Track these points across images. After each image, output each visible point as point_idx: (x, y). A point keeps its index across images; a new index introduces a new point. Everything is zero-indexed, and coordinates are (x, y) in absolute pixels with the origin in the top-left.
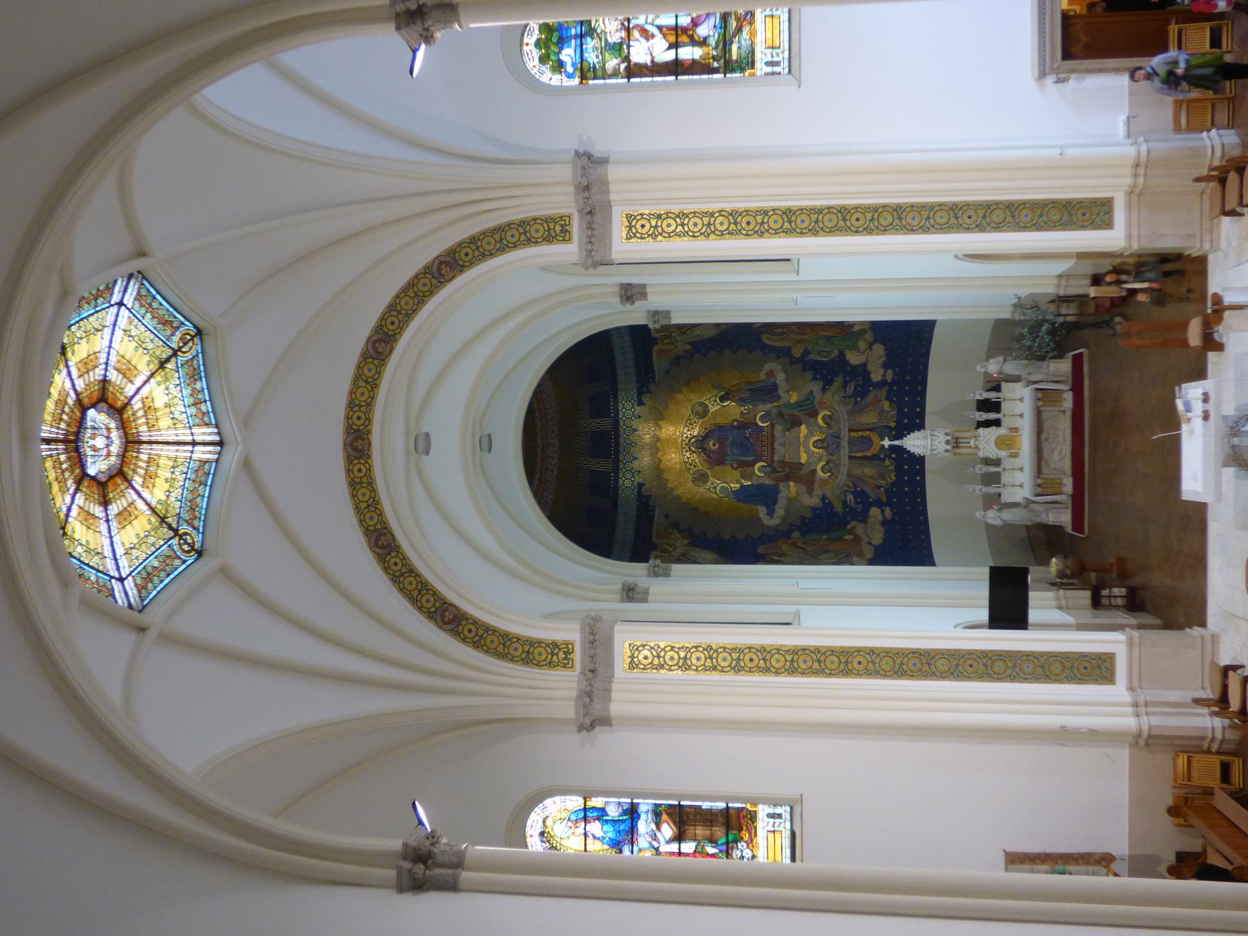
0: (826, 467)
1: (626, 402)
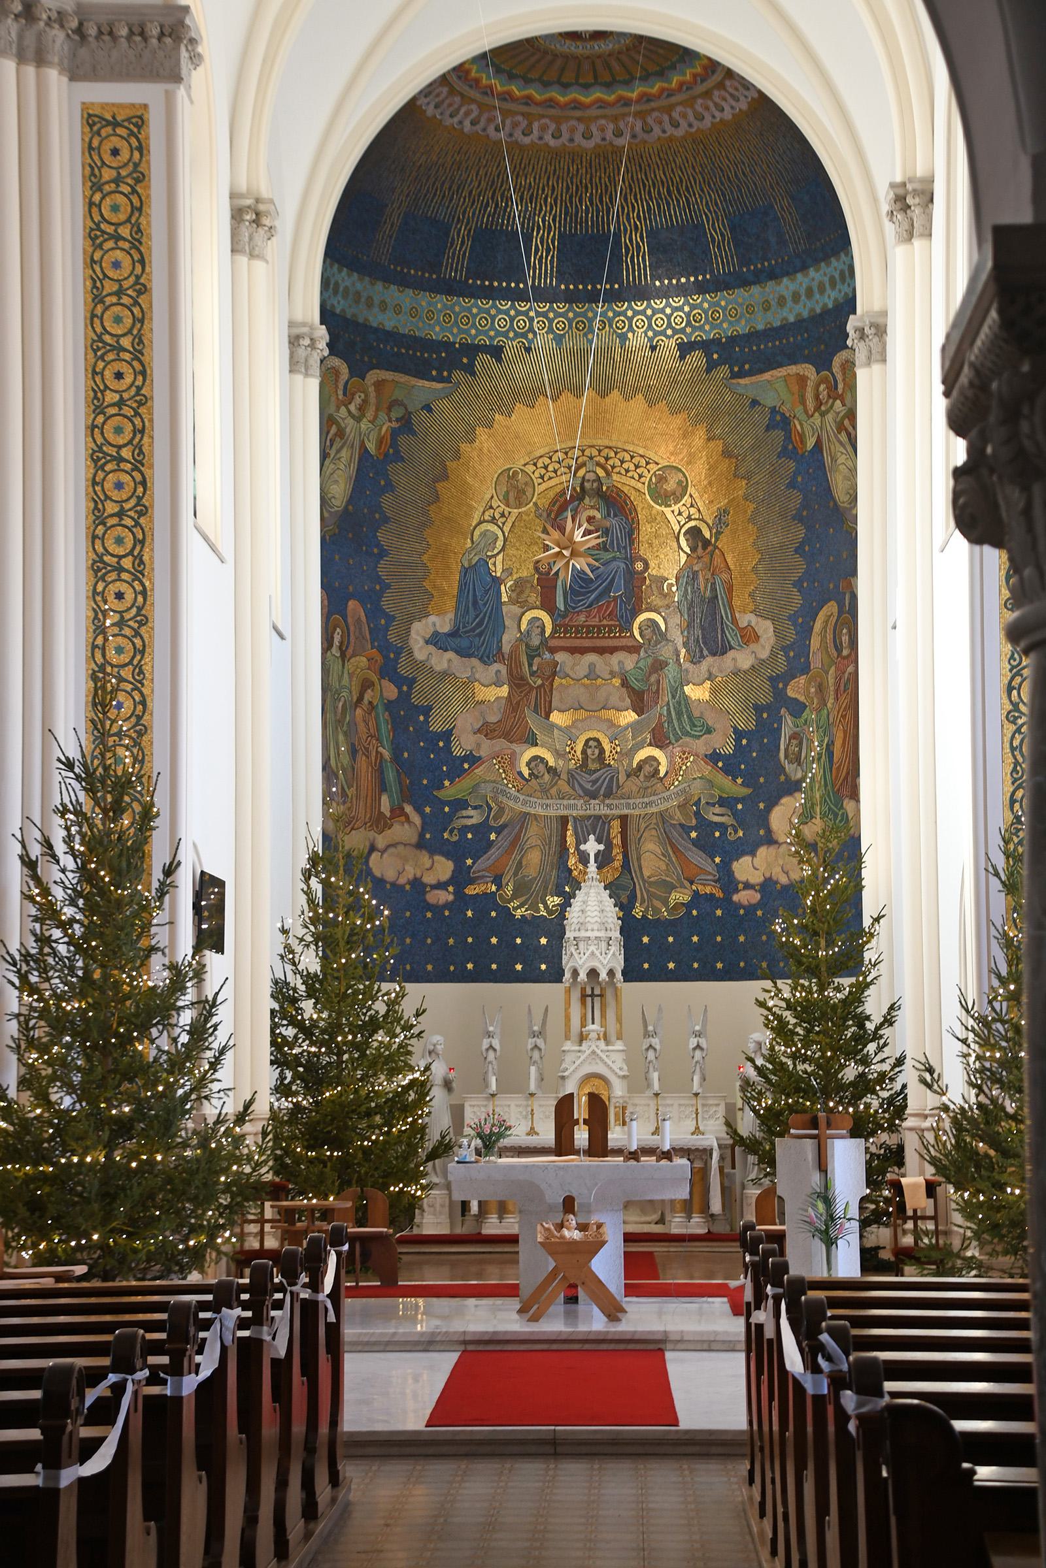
0: (542, 767)
1: (688, 315)
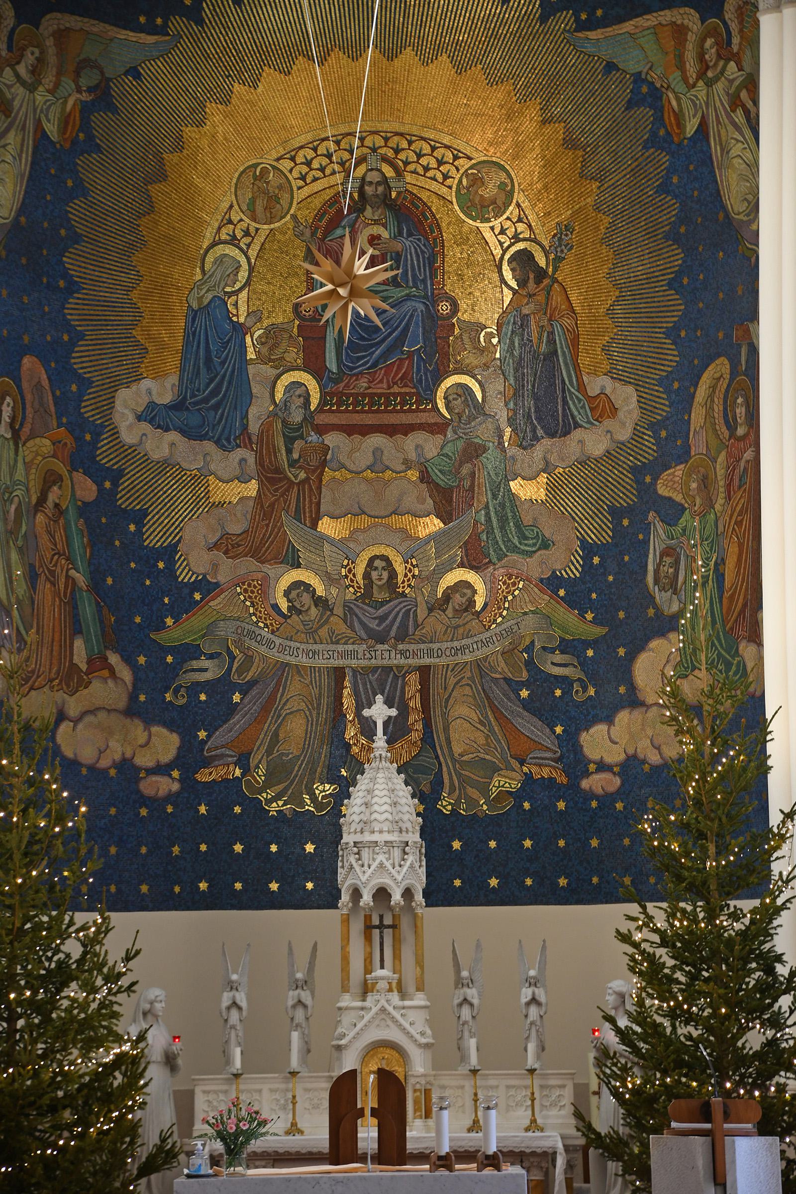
0: (306, 598)
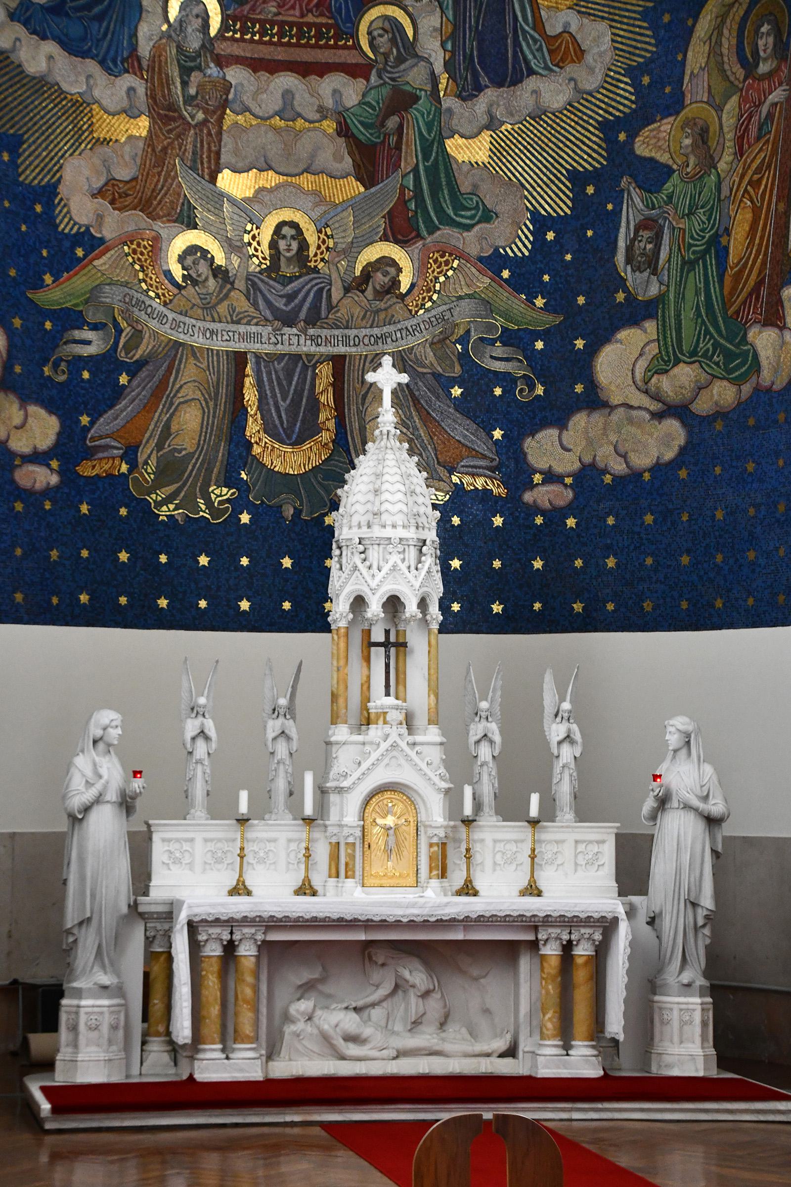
0: (203, 268)
